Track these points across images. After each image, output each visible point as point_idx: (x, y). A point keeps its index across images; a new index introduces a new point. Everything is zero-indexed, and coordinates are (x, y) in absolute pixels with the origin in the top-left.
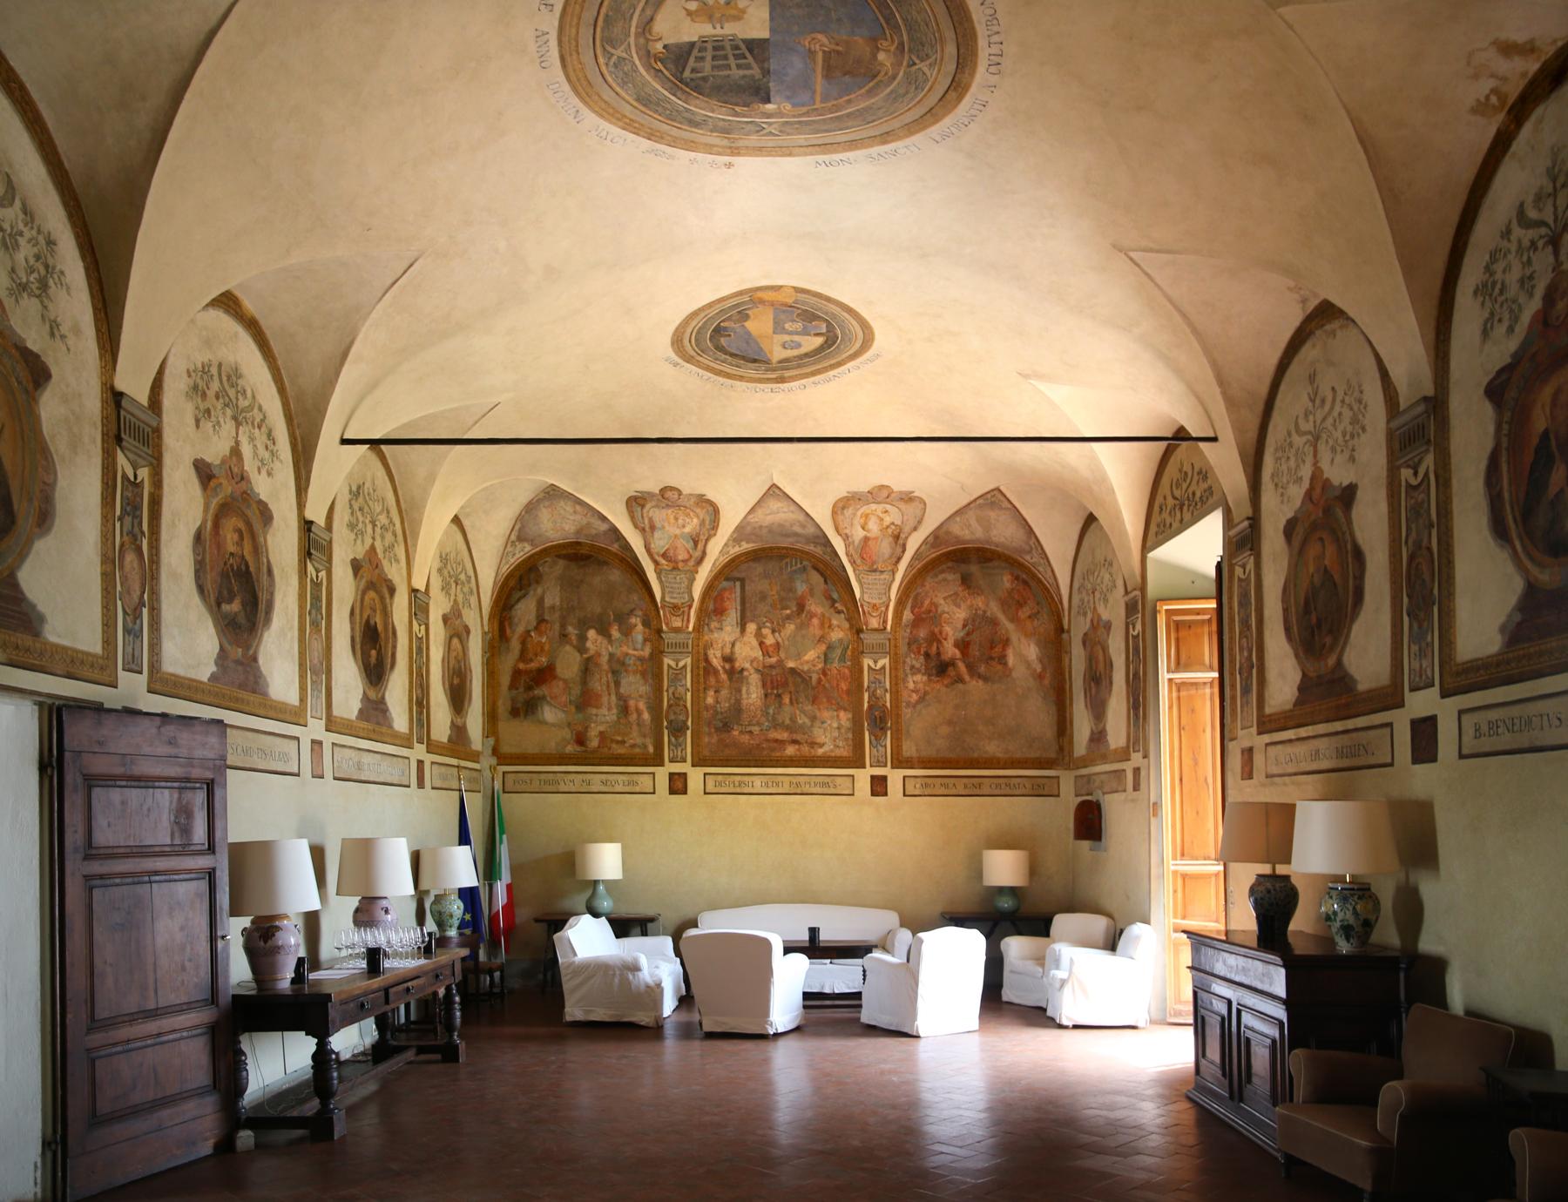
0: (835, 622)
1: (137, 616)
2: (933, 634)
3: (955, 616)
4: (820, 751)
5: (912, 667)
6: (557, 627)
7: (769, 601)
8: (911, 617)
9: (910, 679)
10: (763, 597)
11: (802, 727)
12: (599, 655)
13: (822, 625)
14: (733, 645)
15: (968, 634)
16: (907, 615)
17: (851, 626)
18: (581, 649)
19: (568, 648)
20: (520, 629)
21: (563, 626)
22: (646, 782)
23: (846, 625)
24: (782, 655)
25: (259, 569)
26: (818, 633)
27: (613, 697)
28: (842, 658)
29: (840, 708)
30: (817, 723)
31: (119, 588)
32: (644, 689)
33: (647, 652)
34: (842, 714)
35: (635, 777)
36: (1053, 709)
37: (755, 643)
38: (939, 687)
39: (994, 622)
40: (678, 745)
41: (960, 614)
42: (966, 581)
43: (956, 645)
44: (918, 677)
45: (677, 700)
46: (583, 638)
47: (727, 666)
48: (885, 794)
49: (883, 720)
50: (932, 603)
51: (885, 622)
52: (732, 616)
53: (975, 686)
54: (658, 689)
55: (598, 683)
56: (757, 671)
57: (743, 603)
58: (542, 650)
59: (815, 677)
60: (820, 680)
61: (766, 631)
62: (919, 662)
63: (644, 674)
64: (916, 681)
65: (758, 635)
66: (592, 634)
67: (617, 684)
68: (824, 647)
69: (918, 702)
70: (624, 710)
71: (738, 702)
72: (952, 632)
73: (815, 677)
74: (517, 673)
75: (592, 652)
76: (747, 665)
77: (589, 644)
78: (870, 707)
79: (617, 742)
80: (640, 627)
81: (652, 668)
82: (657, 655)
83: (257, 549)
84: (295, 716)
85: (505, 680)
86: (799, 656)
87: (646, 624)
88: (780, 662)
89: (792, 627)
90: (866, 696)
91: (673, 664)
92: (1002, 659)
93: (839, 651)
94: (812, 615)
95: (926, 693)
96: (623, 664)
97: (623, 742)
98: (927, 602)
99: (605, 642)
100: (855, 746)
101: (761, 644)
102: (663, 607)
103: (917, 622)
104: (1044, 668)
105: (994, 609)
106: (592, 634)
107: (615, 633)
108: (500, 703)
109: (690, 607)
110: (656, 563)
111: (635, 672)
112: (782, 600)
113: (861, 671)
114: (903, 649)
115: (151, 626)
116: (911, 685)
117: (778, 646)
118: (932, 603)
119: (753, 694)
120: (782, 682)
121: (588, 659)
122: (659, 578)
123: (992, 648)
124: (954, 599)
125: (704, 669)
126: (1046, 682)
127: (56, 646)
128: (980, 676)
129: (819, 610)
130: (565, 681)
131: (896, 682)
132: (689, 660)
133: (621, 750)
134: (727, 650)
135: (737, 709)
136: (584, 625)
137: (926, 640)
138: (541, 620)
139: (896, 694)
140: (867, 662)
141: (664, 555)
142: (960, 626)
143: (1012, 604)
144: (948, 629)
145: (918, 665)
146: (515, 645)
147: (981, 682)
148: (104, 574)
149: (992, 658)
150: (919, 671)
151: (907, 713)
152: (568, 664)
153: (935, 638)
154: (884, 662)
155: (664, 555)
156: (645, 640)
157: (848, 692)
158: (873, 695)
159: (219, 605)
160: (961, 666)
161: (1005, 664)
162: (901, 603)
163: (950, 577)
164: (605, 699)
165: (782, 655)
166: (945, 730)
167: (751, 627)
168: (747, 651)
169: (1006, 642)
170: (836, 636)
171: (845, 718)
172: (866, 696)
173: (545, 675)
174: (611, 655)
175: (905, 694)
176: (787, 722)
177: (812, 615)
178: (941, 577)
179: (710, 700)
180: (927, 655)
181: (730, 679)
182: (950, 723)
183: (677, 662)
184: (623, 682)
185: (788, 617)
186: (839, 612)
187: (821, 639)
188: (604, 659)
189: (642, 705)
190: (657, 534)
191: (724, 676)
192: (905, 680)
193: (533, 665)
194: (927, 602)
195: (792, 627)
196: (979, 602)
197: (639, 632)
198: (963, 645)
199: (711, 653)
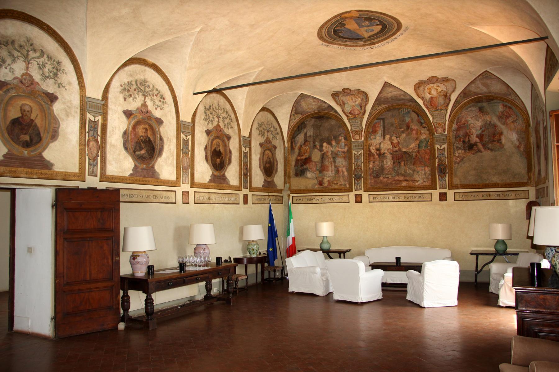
0: (422, 132)
1: (95, 159)
2: (466, 133)
3: (476, 123)
4: (417, 184)
5: (457, 147)
6: (312, 143)
7: (395, 125)
8: (456, 127)
9: (456, 152)
10: (392, 125)
11: (409, 174)
12: (328, 152)
13: (417, 133)
14: (380, 144)
15: (483, 132)
16: (454, 126)
17: (430, 133)
18: (321, 150)
19: (316, 150)
20: (298, 145)
21: (314, 142)
23: (428, 132)
24: (401, 146)
25: (155, 139)
26: (416, 137)
27: (333, 167)
28: (426, 146)
29: (425, 166)
30: (416, 173)
31: (87, 152)
33: (346, 149)
34: (426, 168)
36: (526, 161)
37: (389, 142)
38: (470, 155)
39: (495, 126)
40: (358, 184)
41: (479, 124)
42: (481, 110)
43: (477, 137)
44: (460, 151)
45: (359, 166)
46: (321, 146)
47: (378, 152)
48: (446, 200)
49: (444, 170)
50: (465, 120)
51: (444, 130)
52: (380, 133)
53: (487, 154)
54: (350, 163)
55: (327, 163)
56: (390, 153)
57: (384, 127)
58: (307, 151)
59: (414, 154)
60: (416, 156)
61: (393, 138)
62: (460, 145)
63: (345, 158)
64: (459, 153)
65: (390, 139)
66: (325, 144)
67: (335, 162)
68: (418, 142)
69: (460, 162)
71: (382, 166)
72: (475, 132)
73: (414, 154)
74: (297, 161)
75: (325, 151)
76: (386, 152)
77: (324, 148)
78: (439, 165)
79: (335, 184)
80: (343, 140)
81: (348, 155)
82: (349, 151)
83: (154, 133)
84: (176, 183)
85: (293, 163)
86: (407, 146)
87: (346, 139)
88: (400, 149)
89: (405, 135)
90: (437, 160)
91: (356, 153)
92: (499, 141)
93: (425, 143)
94: (412, 130)
95: (464, 157)
96: (337, 154)
98: (463, 120)
100: (432, 181)
101: (392, 143)
103: (458, 129)
104: (520, 143)
105: (495, 120)
106: (325, 144)
107: (334, 143)
108: (291, 171)
109: (362, 131)
111: (341, 158)
112: (400, 125)
113: (435, 150)
114: (453, 140)
115: (101, 162)
116: (457, 155)
117: (399, 143)
118: (465, 120)
119: (388, 163)
120: (400, 157)
121: (323, 154)
123: (494, 137)
124: (476, 118)
125: (369, 154)
126: (522, 149)
127: (58, 172)
128: (489, 149)
129: (416, 127)
130: (315, 162)
131: (450, 154)
132: (362, 151)
134: (378, 146)
135: (382, 169)
136: (322, 141)
137: (463, 136)
138: (306, 141)
139: (450, 158)
140: (437, 147)
142: (478, 128)
143: (504, 117)
144: (473, 130)
145: (460, 146)
146: (297, 150)
147: (489, 152)
148: (80, 150)
149: (494, 141)
150: (460, 149)
151: (455, 166)
152: (316, 156)
153: (467, 135)
154: (445, 146)
156: (345, 145)
157: (429, 159)
158: (440, 160)
159: (134, 152)
160: (480, 146)
161: (501, 143)
162: (451, 122)
163: (473, 109)
164: (330, 168)
165: (401, 146)
166: (473, 172)
167: (388, 137)
168: (386, 146)
169: (501, 134)
170: (423, 137)
171: (428, 170)
172: (437, 160)
173: (308, 160)
175: (454, 159)
176: (403, 173)
177: (412, 130)
178: (469, 109)
179: (371, 166)
180: (464, 142)
181: (379, 157)
182: (475, 169)
183: (358, 152)
184: (337, 161)
185: (403, 132)
186: (424, 128)
187: (417, 139)
188: (330, 153)
191: (376, 156)
192: (454, 153)
193: (303, 157)
194: (463, 120)
195: (405, 135)
196: (488, 118)
198: (480, 137)
199: (371, 148)
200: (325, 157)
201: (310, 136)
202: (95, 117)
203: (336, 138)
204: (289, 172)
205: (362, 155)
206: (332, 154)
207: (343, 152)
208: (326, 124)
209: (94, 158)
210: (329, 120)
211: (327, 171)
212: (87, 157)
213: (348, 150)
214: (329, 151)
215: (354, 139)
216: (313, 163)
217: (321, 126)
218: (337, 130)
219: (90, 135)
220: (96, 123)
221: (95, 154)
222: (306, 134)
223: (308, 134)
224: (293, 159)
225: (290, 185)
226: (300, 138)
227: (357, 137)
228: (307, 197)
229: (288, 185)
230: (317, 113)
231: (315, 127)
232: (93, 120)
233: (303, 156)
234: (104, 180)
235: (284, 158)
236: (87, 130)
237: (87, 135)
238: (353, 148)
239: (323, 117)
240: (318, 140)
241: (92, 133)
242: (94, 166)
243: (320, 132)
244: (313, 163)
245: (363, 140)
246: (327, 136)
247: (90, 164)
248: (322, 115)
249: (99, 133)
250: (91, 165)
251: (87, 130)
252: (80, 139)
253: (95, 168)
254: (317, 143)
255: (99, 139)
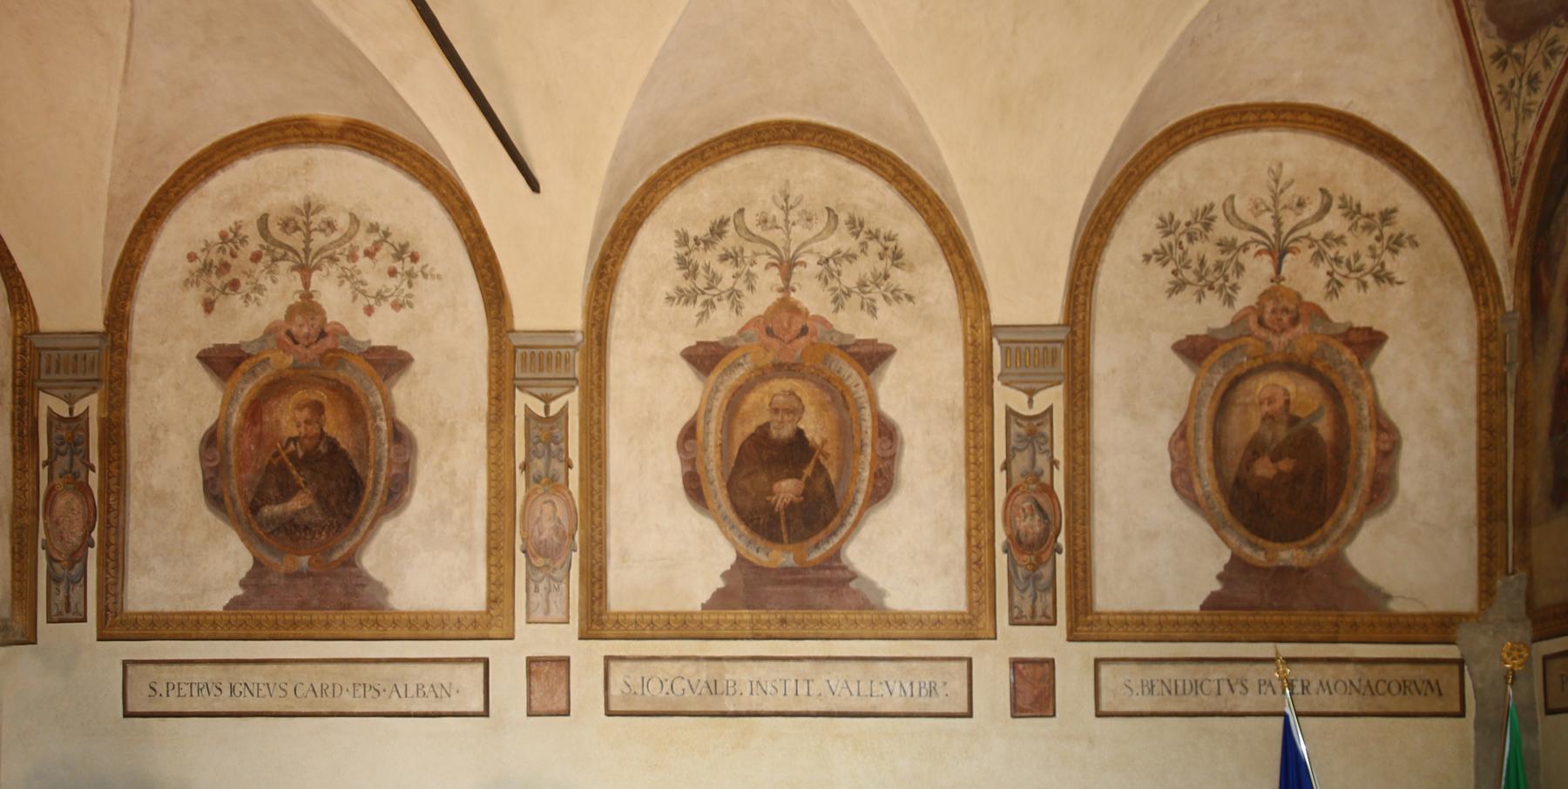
1: (77, 557)
31: (42, 535)
115: (103, 566)
202: (71, 401)
209: (74, 553)
212: (42, 554)
219: (56, 474)
220: (80, 422)
221: (75, 540)
232: (67, 415)
234: (116, 631)
236: (44, 455)
237: (44, 473)
241: (62, 462)
242: (72, 582)
247: (53, 578)
249: (94, 459)
250: (58, 581)
251: (44, 455)
252: (19, 491)
253: (78, 588)
255: (94, 480)
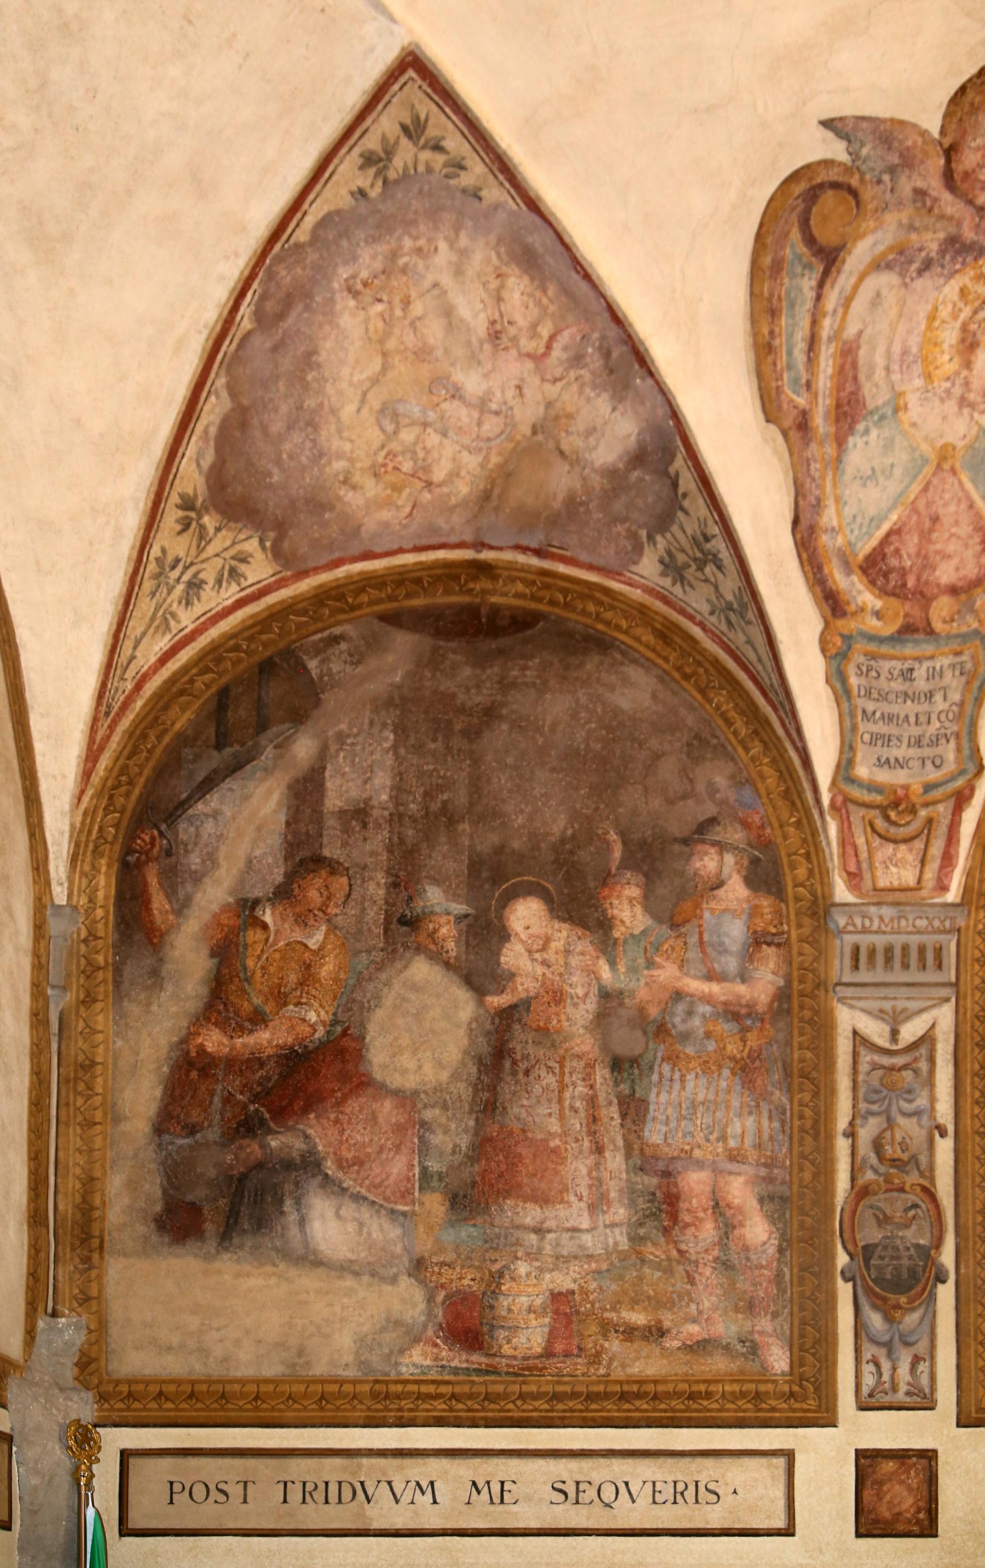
6: (376, 887)
12: (558, 997)
18: (478, 968)
20: (213, 895)
21: (403, 882)
22: (751, 1490)
27: (615, 1161)
32: (745, 1127)
33: (763, 983)
35: (707, 1470)
55: (547, 1109)
63: (746, 1069)
66: (526, 916)
67: (633, 1109)
70: (663, 1207)
74: (190, 1071)
75: (525, 986)
77: (513, 956)
85: (141, 1097)
87: (764, 875)
91: (876, 1031)
96: (661, 1030)
97: (657, 1333)
99: (584, 945)
102: (842, 806)
106: (526, 916)
107: (628, 910)
110: (832, 603)
111: (708, 1067)
121: (508, 1015)
122: (837, 679)
130: (407, 1099)
132: (945, 1017)
133: (646, 1364)
136: (494, 880)
138: (305, 858)
141: (875, 567)
152: (420, 1031)
155: (875, 567)
156: (758, 940)
164: (578, 1169)
173: (320, 1072)
174: (609, 999)
188: (578, 1016)
189: (740, 1190)
190: (863, 450)
193: (266, 1039)
197: (732, 908)
200: (521, 1041)
201: (359, 814)
203: (652, 857)
204: (90, 1183)
205: (944, 1051)
206: (601, 1018)
207: (734, 1013)
208: (558, 707)
210: (592, 663)
211: (543, 1200)
213: (783, 996)
214: (577, 985)
215: (853, 878)
216: (387, 1109)
217: (490, 713)
218: (668, 771)
222: (306, 790)
223: (338, 792)
224: (143, 1044)
225: (99, 1331)
226: (241, 826)
227: (897, 868)
228: (298, 1469)
229: (68, 1331)
230: (449, 574)
231: (420, 718)
233: (258, 1019)
235: (38, 1019)
238: (839, 968)
239: (521, 622)
240: (444, 858)
243: (476, 784)
244: (387, 1109)
245: (953, 895)
246: (558, 824)
248: (505, 597)
254: (434, 896)
